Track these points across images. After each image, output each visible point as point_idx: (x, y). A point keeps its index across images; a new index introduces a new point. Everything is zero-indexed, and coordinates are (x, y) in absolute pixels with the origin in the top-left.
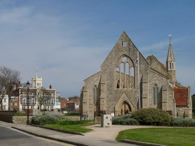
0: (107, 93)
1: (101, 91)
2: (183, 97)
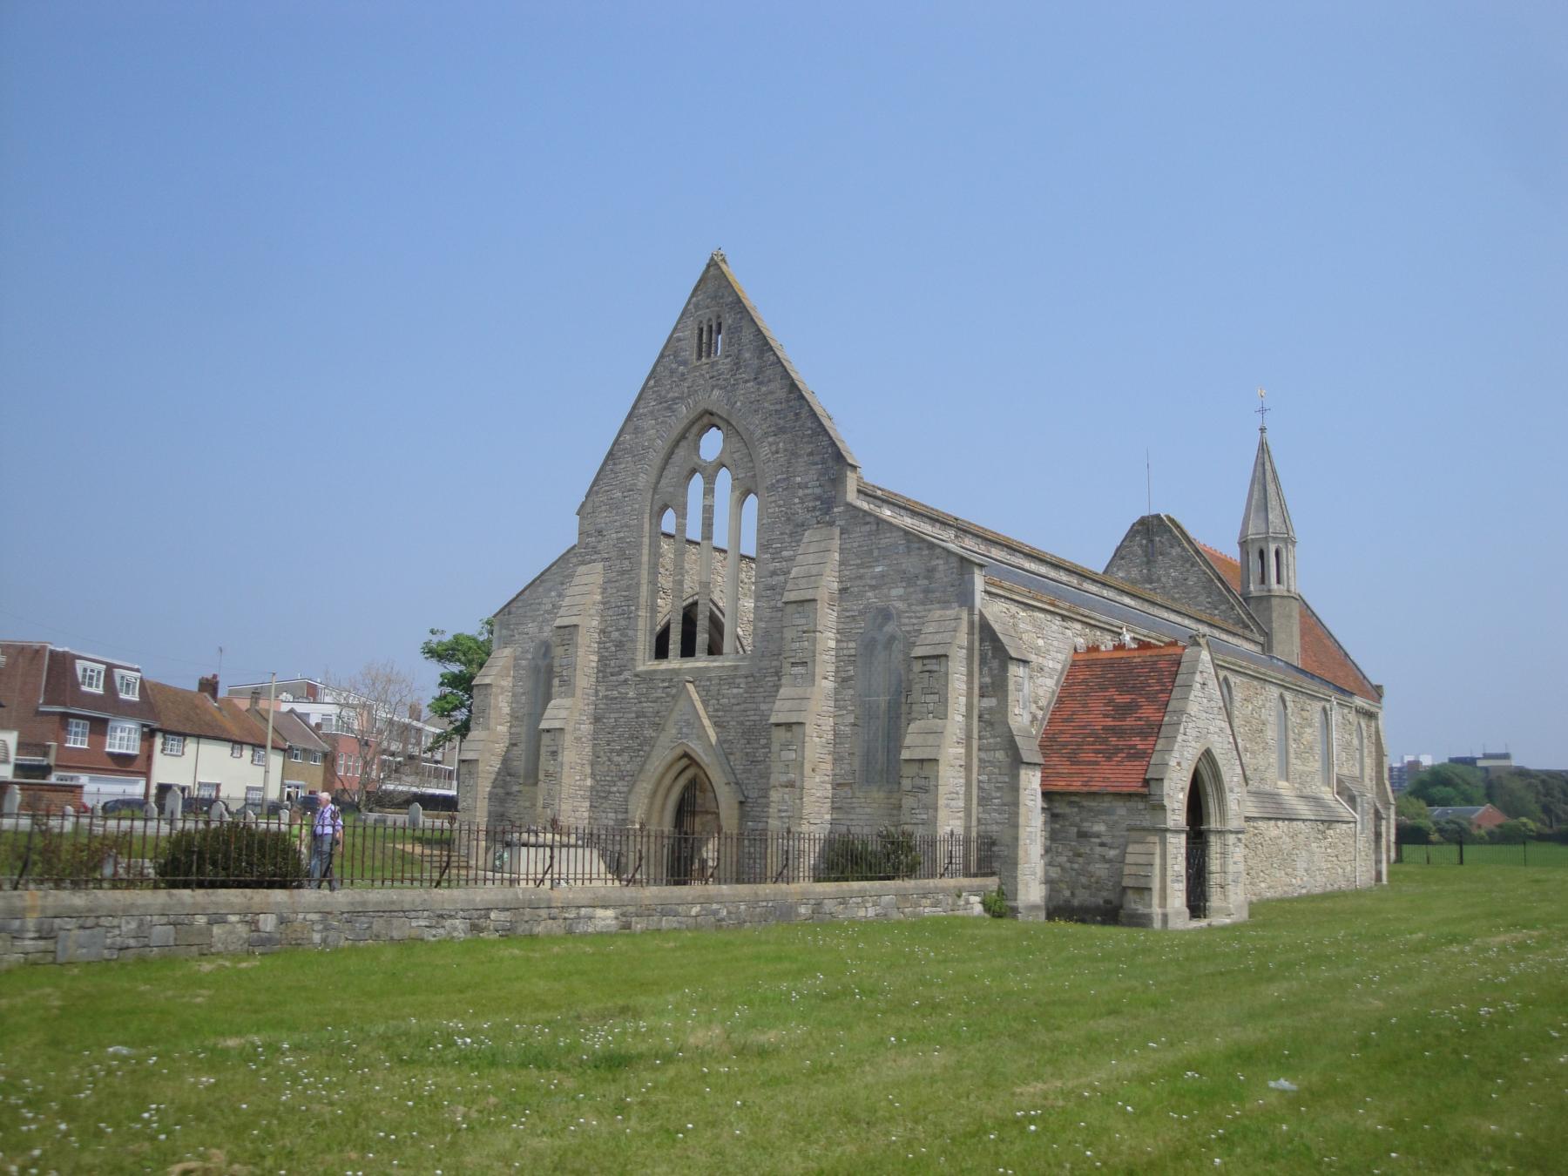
1: (556, 682)
2: (1129, 722)
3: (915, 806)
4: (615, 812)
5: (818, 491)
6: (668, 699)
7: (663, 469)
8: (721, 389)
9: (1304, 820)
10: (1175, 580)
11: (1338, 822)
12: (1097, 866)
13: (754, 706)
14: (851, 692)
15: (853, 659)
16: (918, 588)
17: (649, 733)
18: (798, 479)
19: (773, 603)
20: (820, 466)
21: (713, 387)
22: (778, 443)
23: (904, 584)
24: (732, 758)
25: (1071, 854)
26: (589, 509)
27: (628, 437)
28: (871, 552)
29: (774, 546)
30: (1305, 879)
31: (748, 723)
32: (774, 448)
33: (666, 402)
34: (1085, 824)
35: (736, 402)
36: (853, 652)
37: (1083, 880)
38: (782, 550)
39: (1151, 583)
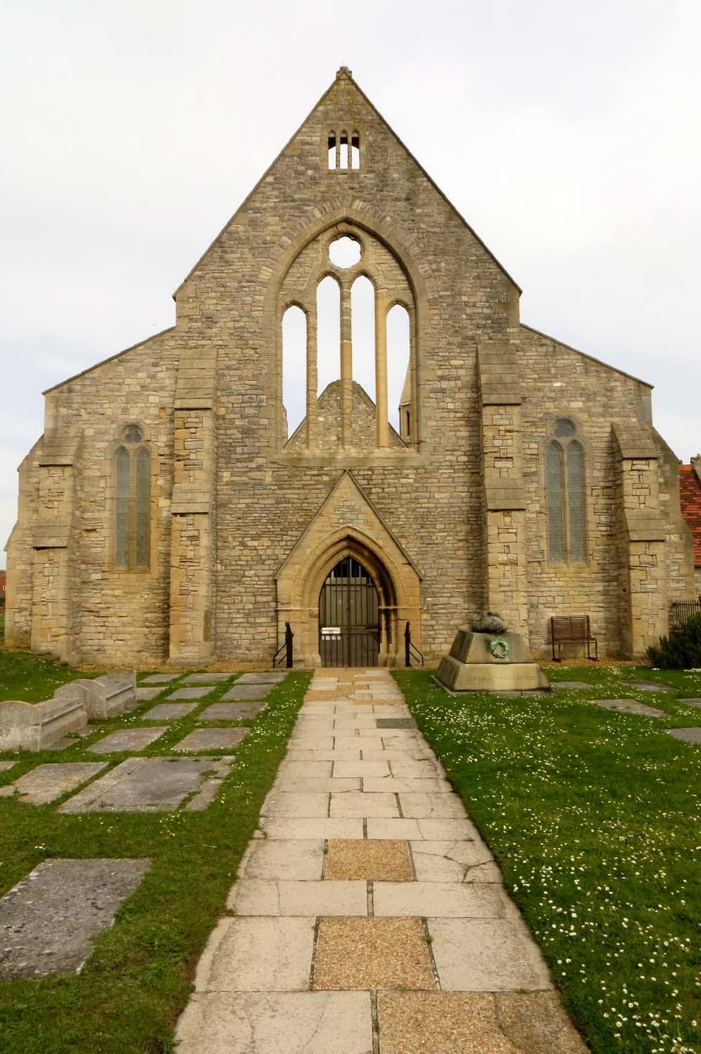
0: (216, 477)
3: (644, 578)
4: (254, 596)
5: (487, 311)
6: (318, 486)
8: (365, 201)
10: (361, 427)
13: (428, 495)
14: (535, 485)
15: (535, 457)
16: (598, 404)
18: (465, 298)
19: (442, 405)
20: (489, 290)
21: (355, 198)
22: (439, 263)
24: (403, 541)
26: (190, 291)
27: (241, 228)
28: (549, 369)
29: (441, 354)
31: (421, 510)
32: (434, 266)
33: (293, 201)
35: (385, 217)
36: (535, 452)
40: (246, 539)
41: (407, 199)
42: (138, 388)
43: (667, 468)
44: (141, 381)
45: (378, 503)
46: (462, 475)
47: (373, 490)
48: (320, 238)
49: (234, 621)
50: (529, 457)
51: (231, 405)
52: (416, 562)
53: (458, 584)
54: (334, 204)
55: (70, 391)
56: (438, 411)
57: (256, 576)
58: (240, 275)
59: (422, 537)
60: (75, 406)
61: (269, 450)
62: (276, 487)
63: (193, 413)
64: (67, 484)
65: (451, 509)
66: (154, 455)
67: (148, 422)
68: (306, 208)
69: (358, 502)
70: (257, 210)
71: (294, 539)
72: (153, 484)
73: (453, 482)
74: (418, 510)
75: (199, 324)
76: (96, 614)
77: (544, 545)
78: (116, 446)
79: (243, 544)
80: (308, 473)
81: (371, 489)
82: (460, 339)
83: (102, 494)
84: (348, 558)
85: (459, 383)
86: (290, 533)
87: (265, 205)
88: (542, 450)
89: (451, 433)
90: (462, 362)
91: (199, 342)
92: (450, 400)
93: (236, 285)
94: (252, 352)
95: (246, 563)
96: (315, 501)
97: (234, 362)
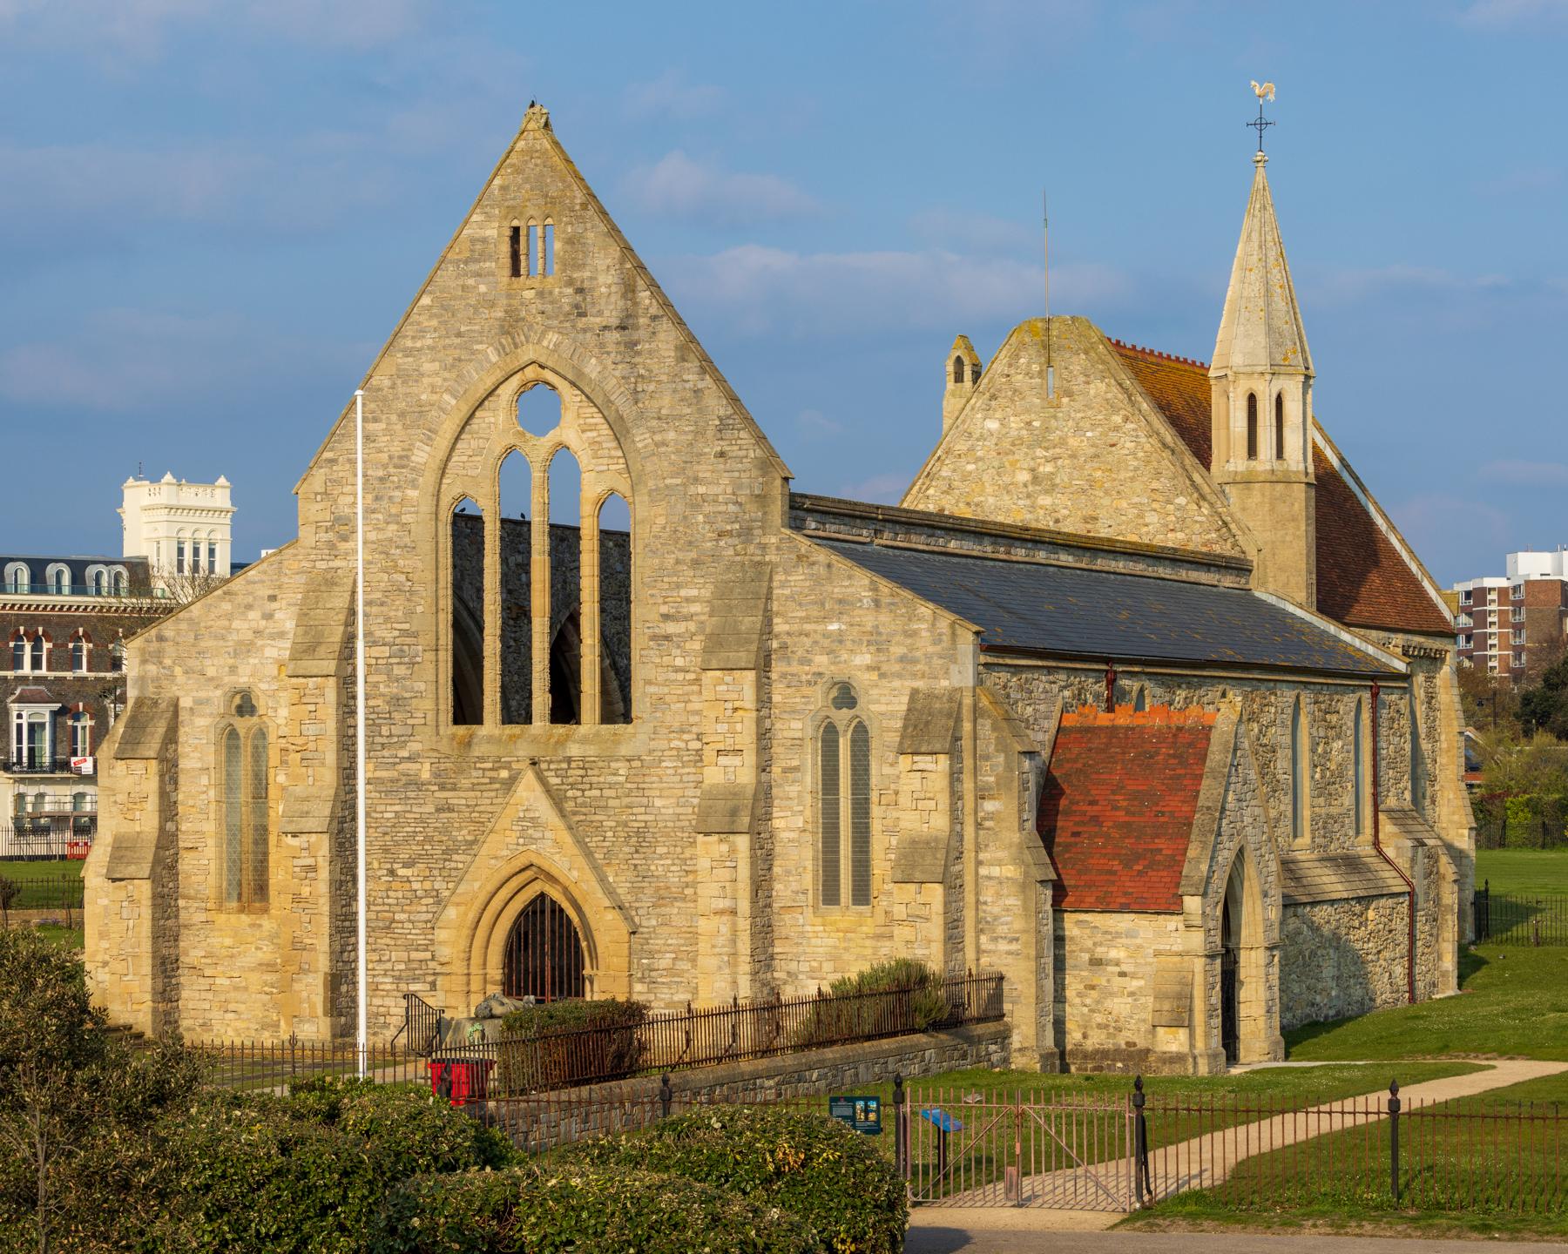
6: (497, 786)
7: (457, 439)
9: (1332, 902)
11: (1382, 896)
12: (1116, 1000)
13: (645, 800)
15: (797, 742)
17: (463, 835)
18: (701, 490)
21: (549, 328)
23: (872, 649)
25: (1081, 987)
30: (1333, 993)
31: (636, 825)
32: (658, 438)
34: (1099, 950)
36: (799, 735)
37: (1098, 1018)
38: (678, 586)
39: (1047, 449)
40: (395, 866)
41: (622, 328)
42: (250, 635)
43: (1001, 759)
44: (254, 625)
45: (575, 813)
46: (693, 770)
47: (570, 793)
48: (499, 391)
49: (380, 987)
50: (790, 742)
51: (373, 661)
52: (627, 905)
53: (686, 939)
54: (517, 340)
55: (161, 639)
56: (660, 670)
57: (410, 921)
58: (386, 455)
59: (635, 866)
60: (168, 662)
61: (426, 729)
62: (436, 788)
63: (311, 682)
64: (152, 785)
65: (678, 824)
66: (272, 738)
67: (264, 686)
68: (476, 347)
69: (543, 809)
70: (408, 352)
71: (460, 866)
72: (271, 781)
73: (681, 781)
74: (631, 824)
75: (331, 536)
76: (200, 973)
77: (808, 880)
78: (223, 723)
79: (392, 872)
80: (478, 765)
81: (566, 791)
82: (693, 555)
83: (203, 796)
84: (542, 896)
85: (692, 626)
86: (455, 857)
87: (419, 344)
88: (810, 732)
89: (679, 705)
90: (694, 592)
91: (331, 564)
92: (678, 652)
93: (381, 473)
94: (402, 578)
95: (395, 902)
96: (490, 809)
97: (379, 595)
